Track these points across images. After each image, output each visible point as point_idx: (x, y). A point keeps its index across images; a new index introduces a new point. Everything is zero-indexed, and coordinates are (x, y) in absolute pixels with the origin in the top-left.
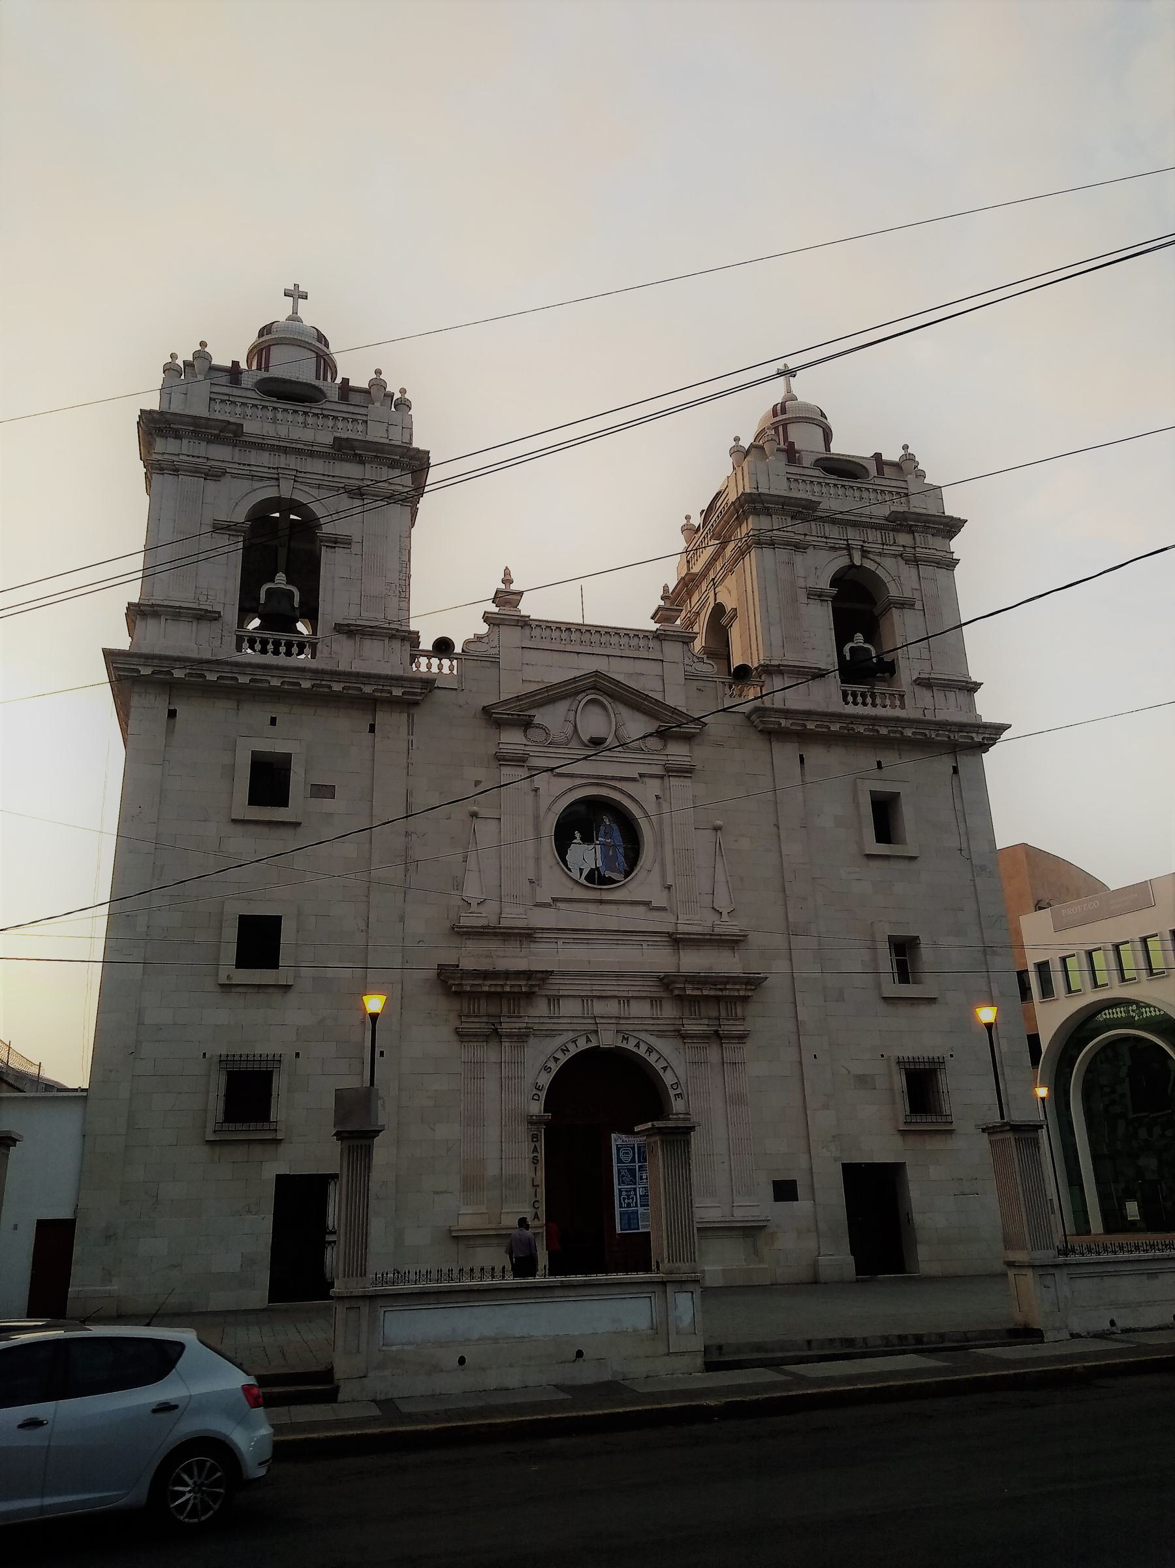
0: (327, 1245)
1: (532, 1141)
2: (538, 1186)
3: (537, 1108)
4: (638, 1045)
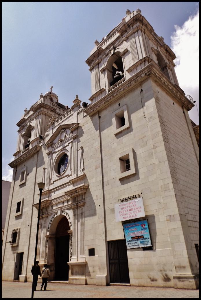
3: (48, 234)
4: (65, 213)
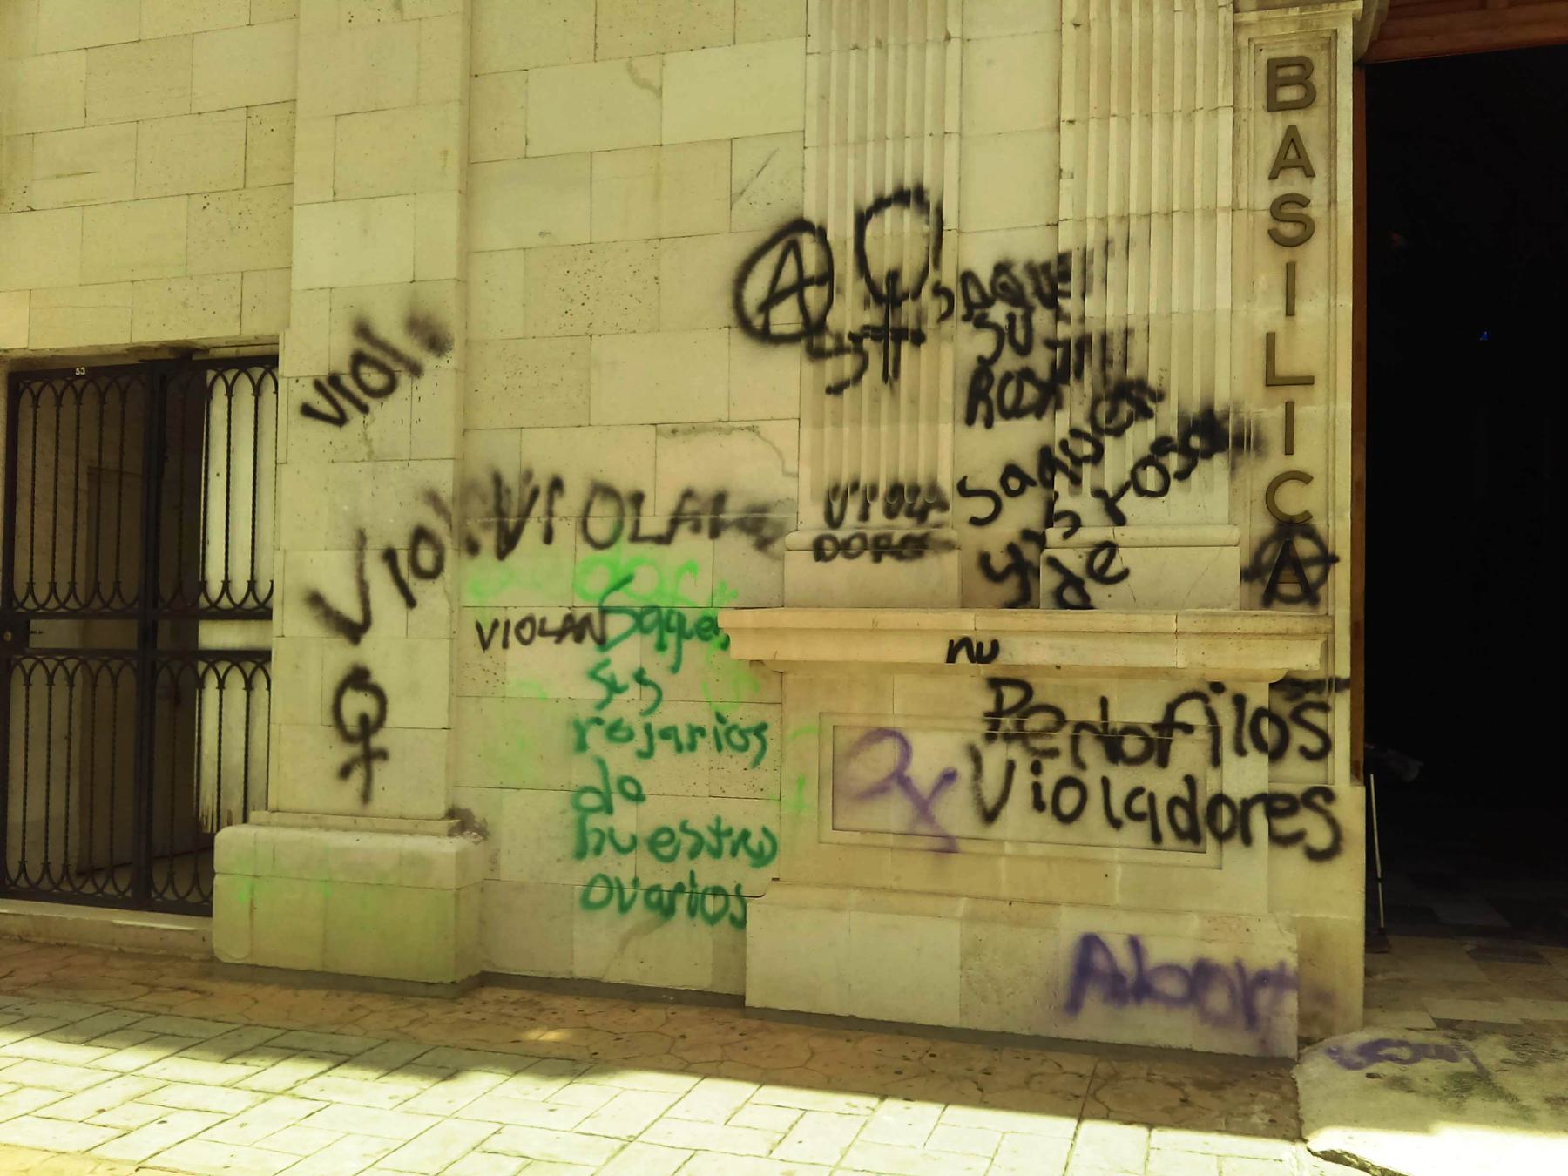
0: (202, 666)
1: (1274, 106)
2: (1308, 381)
